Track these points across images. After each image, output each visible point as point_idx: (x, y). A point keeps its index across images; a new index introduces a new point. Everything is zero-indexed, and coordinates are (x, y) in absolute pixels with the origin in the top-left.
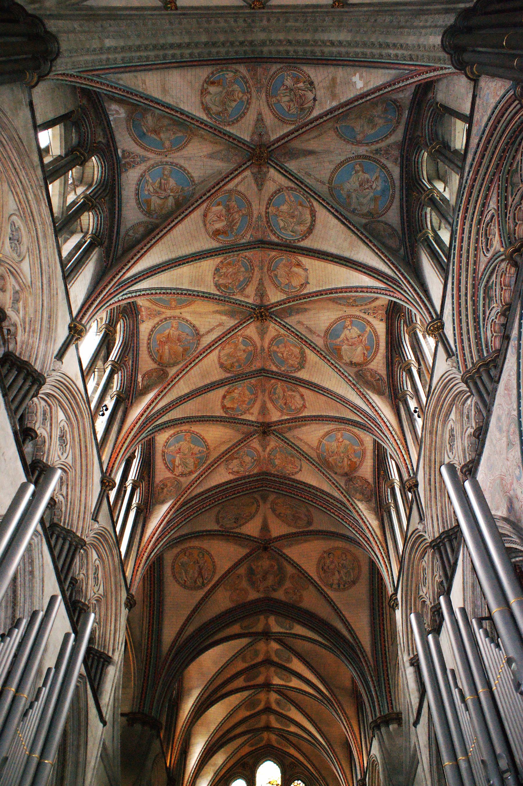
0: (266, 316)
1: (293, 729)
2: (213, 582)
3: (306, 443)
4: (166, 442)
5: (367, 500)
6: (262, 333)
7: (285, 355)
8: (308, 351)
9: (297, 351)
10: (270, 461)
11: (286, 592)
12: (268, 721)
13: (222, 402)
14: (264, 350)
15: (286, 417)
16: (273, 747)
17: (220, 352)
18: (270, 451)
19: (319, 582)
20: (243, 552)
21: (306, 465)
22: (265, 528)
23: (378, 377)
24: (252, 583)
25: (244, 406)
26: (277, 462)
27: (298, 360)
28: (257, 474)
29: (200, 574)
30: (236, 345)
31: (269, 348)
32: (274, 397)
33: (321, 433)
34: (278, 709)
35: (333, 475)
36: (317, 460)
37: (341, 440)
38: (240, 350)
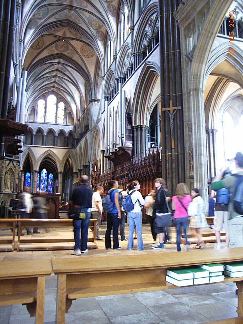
1: (62, 89)
2: (43, 48)
3: (85, 15)
5: (101, 40)
11: (68, 53)
12: (54, 85)
15: (79, 7)
16: (54, 91)
19: (80, 54)
20: (56, 39)
21: (83, 23)
22: (64, 34)
23: (115, 8)
24: (57, 49)
28: (65, 20)
29: (38, 44)
34: (58, 83)
35: (92, 30)
36: (87, 22)
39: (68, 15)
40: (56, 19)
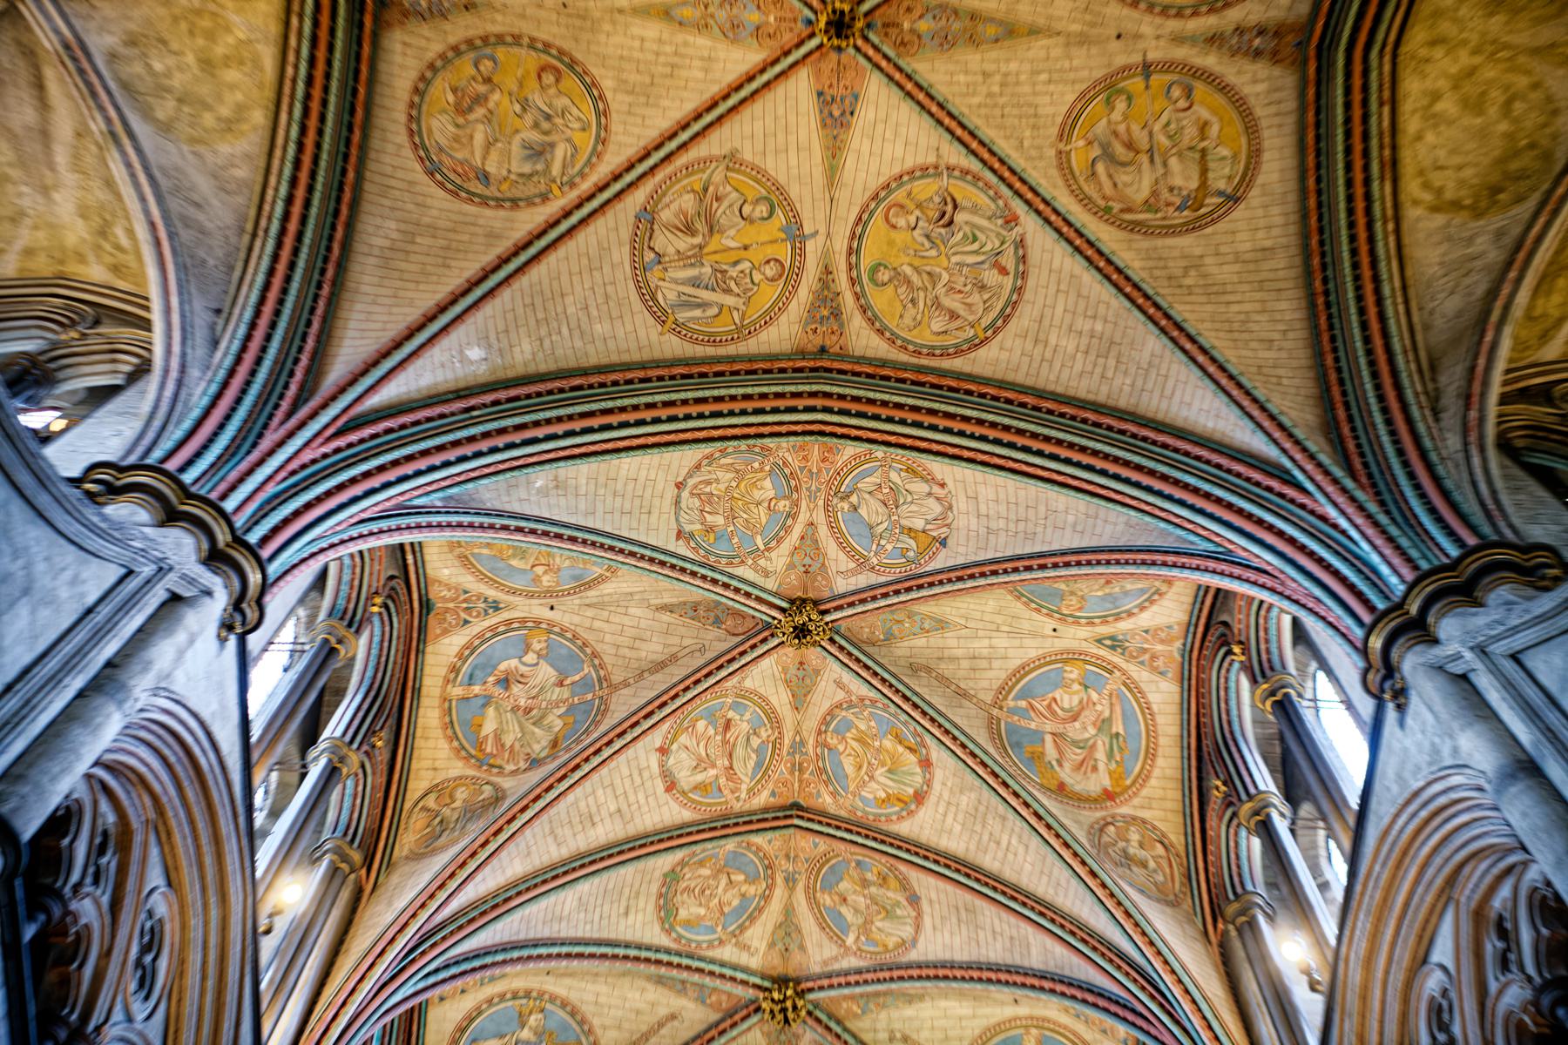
0: (772, 1011)
4: (1152, 602)
6: (788, 927)
7: (724, 881)
8: (654, 935)
9: (689, 909)
10: (791, 485)
13: (929, 783)
14: (787, 880)
15: (729, 684)
17: (915, 941)
18: (788, 530)
25: (863, 727)
26: (767, 489)
27: (683, 885)
30: (865, 928)
31: (771, 887)
32: (764, 734)
33: (608, 588)
37: (539, 570)
38: (856, 911)
39: (812, 497)
40: (929, 478)
